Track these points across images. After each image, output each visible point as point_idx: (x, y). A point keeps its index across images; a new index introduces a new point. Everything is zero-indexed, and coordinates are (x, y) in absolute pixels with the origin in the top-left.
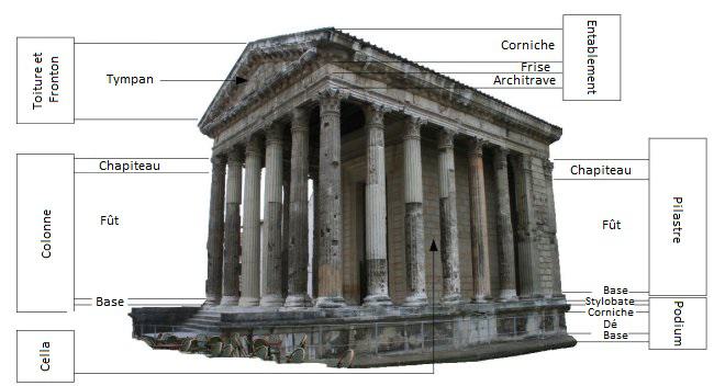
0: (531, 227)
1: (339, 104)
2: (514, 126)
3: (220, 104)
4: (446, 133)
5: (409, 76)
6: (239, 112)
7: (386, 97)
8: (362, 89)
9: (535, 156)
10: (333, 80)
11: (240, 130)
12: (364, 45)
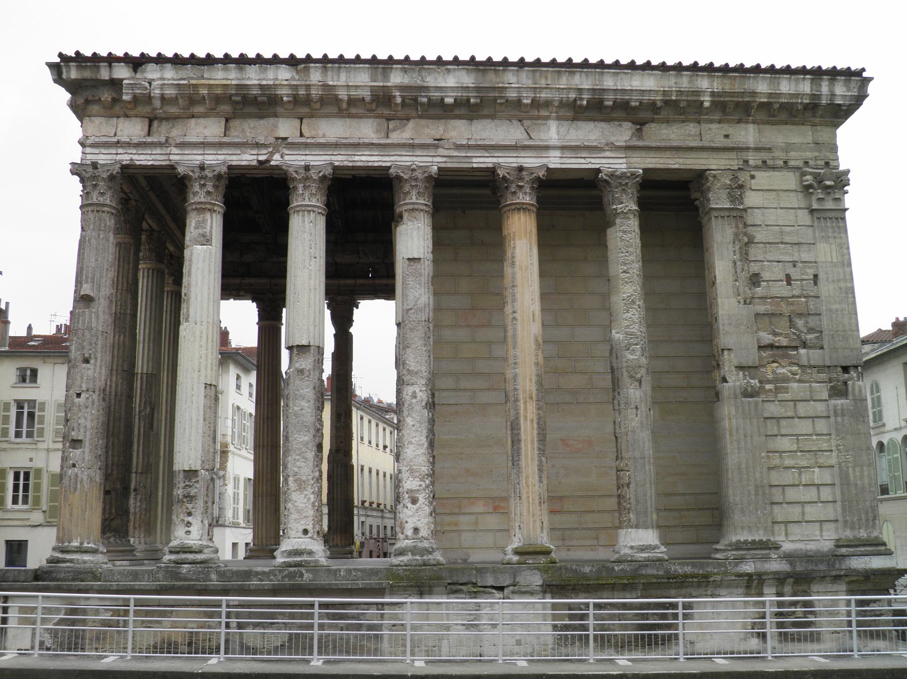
0: (729, 362)
2: (653, 107)
4: (399, 178)
5: (261, 87)
9: (765, 166)
12: (137, 63)
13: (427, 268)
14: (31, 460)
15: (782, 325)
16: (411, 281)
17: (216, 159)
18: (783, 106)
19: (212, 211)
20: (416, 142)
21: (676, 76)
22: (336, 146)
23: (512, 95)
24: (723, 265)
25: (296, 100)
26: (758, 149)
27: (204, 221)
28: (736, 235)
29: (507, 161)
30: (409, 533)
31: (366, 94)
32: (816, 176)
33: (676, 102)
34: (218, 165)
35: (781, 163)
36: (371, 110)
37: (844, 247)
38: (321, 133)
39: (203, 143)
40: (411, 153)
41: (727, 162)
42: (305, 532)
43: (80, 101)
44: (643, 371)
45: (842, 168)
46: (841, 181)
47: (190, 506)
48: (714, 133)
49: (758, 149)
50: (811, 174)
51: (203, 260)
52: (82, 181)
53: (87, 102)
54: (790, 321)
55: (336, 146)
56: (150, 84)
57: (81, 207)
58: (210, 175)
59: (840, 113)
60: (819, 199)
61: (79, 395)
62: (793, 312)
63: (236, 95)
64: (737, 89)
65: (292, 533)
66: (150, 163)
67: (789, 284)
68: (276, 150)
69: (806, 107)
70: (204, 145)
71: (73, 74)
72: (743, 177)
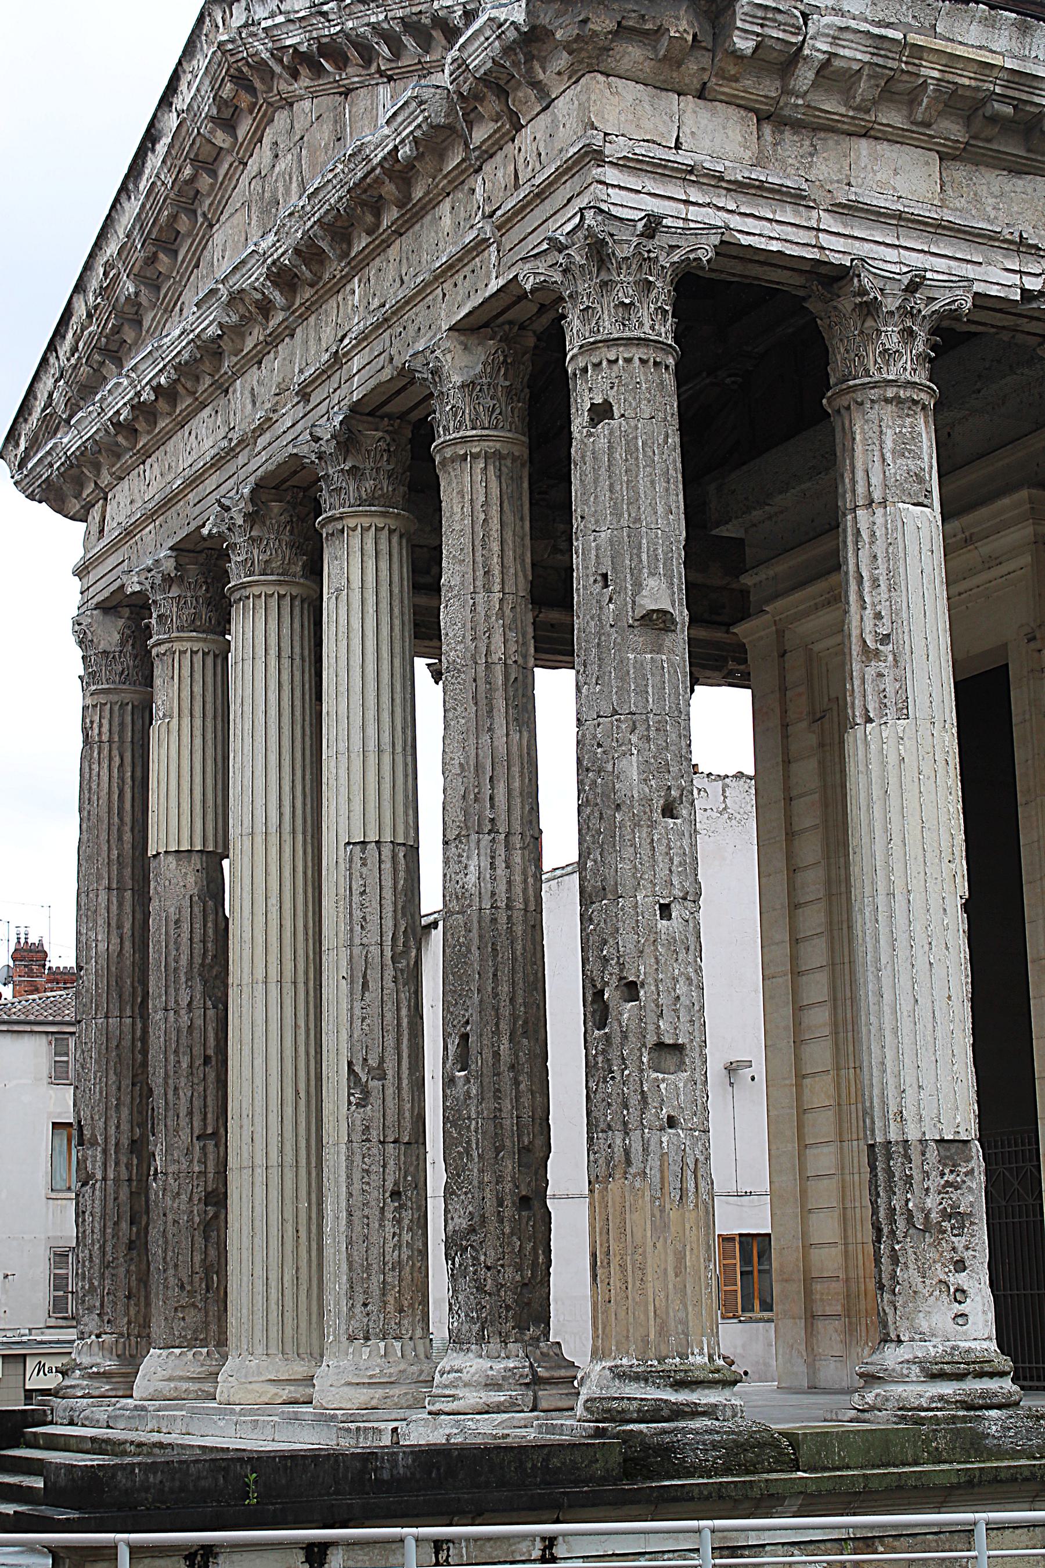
1: (662, 290)
3: (99, 330)
6: (186, 371)
7: (939, 229)
8: (797, 198)
10: (623, 164)
11: (198, 468)
39: (899, 216)
47: (959, 1242)
56: (805, 16)
61: (665, 910)
66: (775, 246)
70: (900, 220)
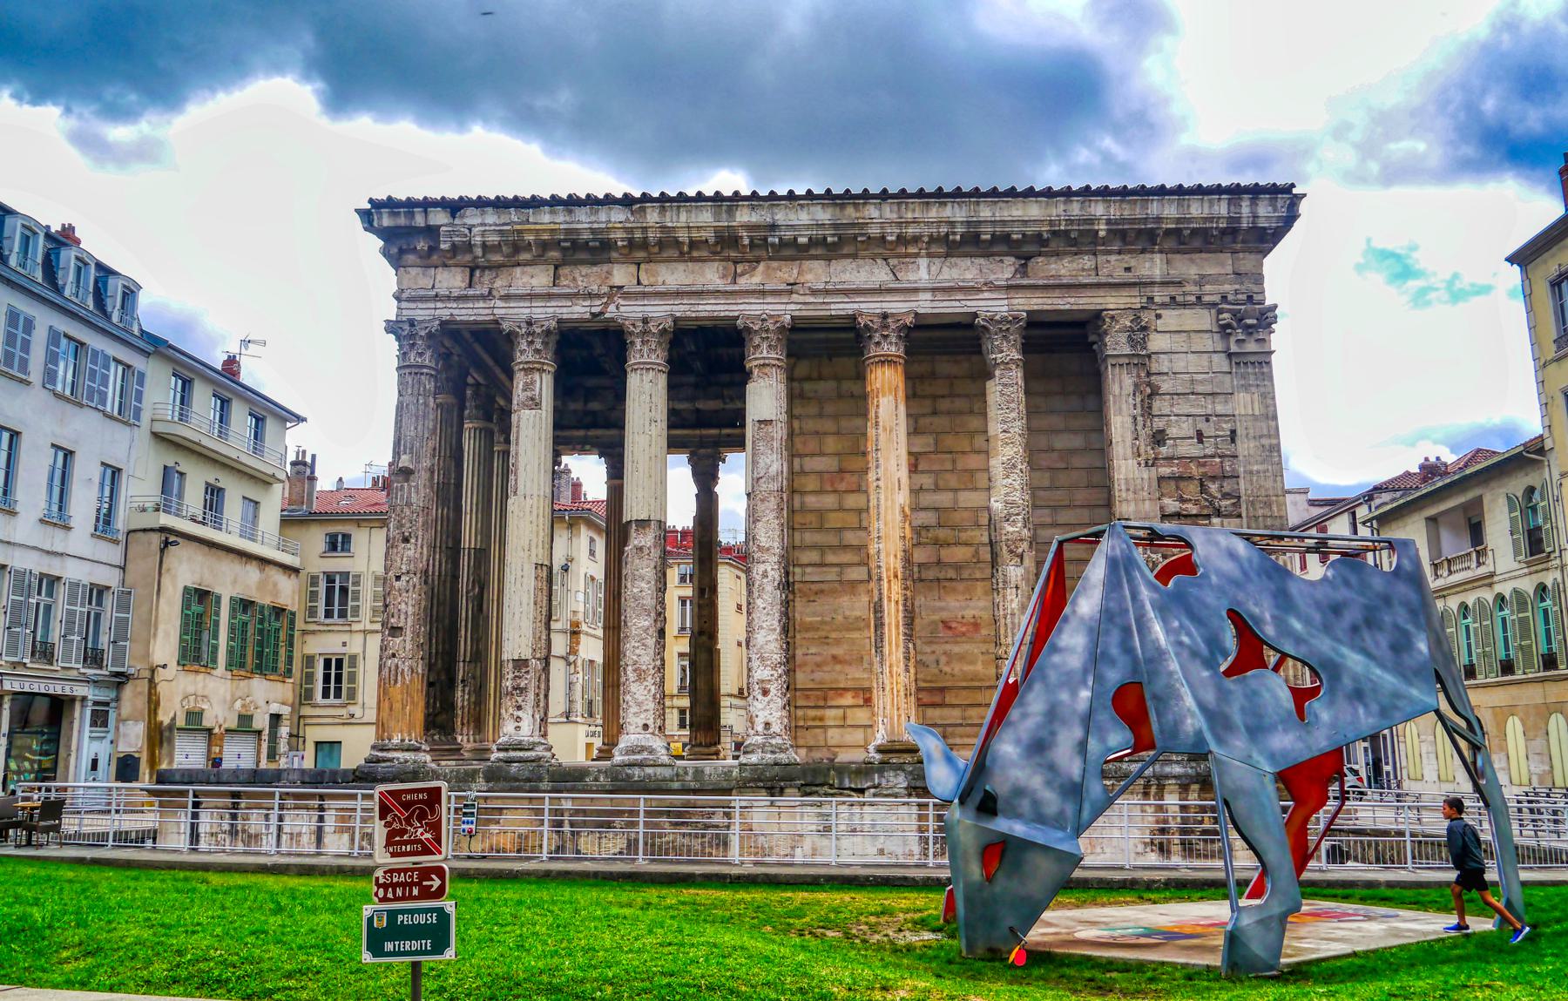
2: (1038, 238)
4: (748, 330)
5: (593, 231)
9: (1173, 303)
12: (455, 207)
13: (779, 432)
14: (344, 644)
15: (1192, 489)
16: (761, 446)
17: (546, 313)
18: (1194, 232)
19: (541, 371)
20: (767, 287)
21: (1065, 203)
22: (678, 294)
23: (874, 231)
24: (1120, 423)
25: (632, 244)
26: (1164, 284)
27: (533, 382)
28: (1136, 385)
29: (869, 307)
30: (760, 728)
31: (709, 235)
32: (1234, 313)
33: (1067, 232)
34: (547, 319)
35: (1193, 299)
36: (715, 253)
37: (1268, 397)
38: (660, 280)
40: (762, 300)
41: (1128, 300)
42: (646, 727)
43: (394, 250)
44: (1025, 545)
45: (1268, 303)
46: (1266, 319)
48: (1114, 266)
49: (1164, 284)
50: (1229, 311)
51: (532, 427)
52: (398, 339)
53: (402, 252)
54: (1202, 485)
55: (678, 294)
57: (399, 368)
58: (538, 330)
59: (1266, 239)
60: (1238, 341)
61: (398, 578)
62: (1205, 474)
63: (565, 240)
64: (1138, 212)
65: (631, 729)
67: (1200, 441)
68: (610, 297)
69: (1223, 232)
70: (531, 297)
71: (387, 221)
72: (1147, 317)
